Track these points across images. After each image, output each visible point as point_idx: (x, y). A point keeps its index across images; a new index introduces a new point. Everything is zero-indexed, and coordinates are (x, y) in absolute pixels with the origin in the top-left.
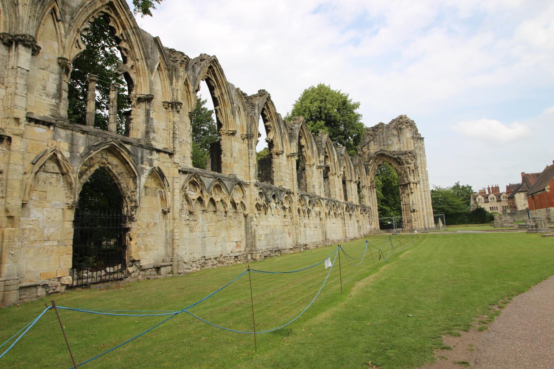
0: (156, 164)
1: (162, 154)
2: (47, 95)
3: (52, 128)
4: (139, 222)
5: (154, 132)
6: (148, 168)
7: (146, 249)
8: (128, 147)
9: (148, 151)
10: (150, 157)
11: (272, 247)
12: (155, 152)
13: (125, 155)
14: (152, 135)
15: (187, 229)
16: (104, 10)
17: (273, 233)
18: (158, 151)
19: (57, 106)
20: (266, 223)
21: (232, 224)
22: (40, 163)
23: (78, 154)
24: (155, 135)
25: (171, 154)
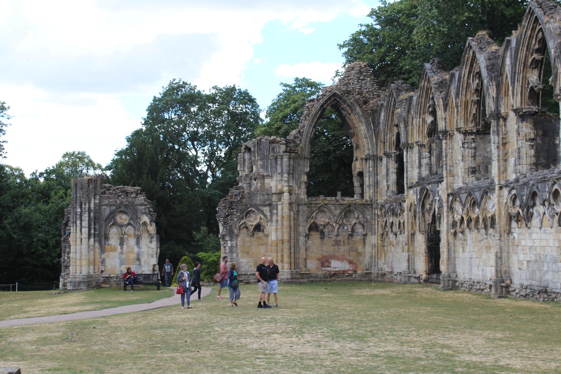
11: (538, 284)
17: (539, 261)
20: (529, 243)
21: (491, 245)
22: (413, 209)
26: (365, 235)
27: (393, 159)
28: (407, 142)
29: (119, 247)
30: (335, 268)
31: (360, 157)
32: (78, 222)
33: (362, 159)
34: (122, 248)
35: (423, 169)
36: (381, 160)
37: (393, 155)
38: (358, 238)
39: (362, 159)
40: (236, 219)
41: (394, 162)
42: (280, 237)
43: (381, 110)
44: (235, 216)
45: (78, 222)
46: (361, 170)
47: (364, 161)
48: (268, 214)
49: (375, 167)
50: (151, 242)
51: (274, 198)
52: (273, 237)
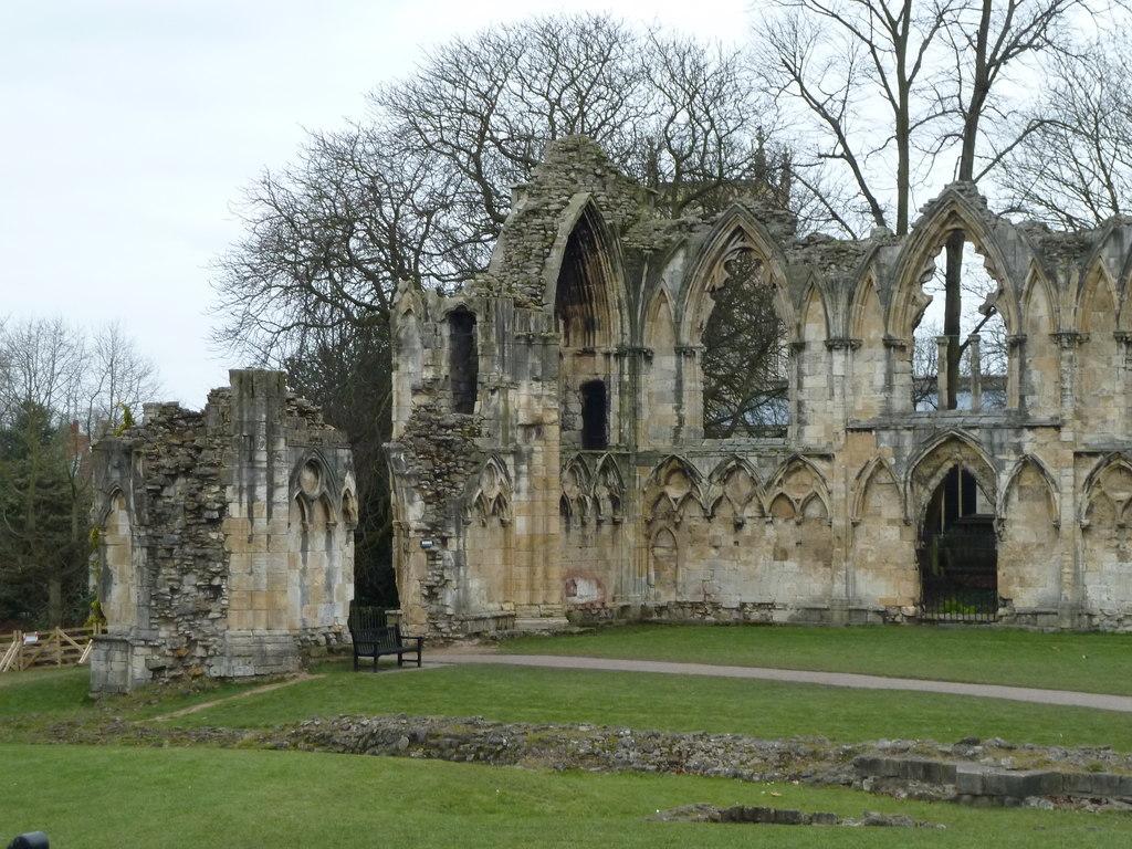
0: (1028, 449)
1: (1040, 431)
2: (875, 391)
3: (874, 433)
4: (1009, 542)
5: (1033, 393)
6: (1013, 457)
7: (1022, 582)
8: (975, 433)
9: (1011, 432)
10: (1016, 441)
12: (1026, 430)
13: (972, 444)
14: (1029, 400)
15: (1114, 556)
16: (949, 227)
18: (1032, 428)
19: (887, 400)
23: (905, 459)
24: (1036, 398)
25: (1058, 428)
26: (616, 523)
27: (698, 360)
28: (847, 334)
29: (300, 555)
30: (582, 597)
31: (603, 349)
32: (261, 491)
33: (607, 355)
34: (304, 561)
35: (897, 393)
36: (648, 357)
37: (698, 353)
38: (606, 529)
39: (607, 355)
40: (462, 485)
41: (698, 368)
42: (539, 530)
43: (674, 255)
44: (460, 478)
45: (261, 491)
46: (601, 378)
47: (612, 358)
48: (512, 474)
49: (634, 373)
50: (347, 543)
51: (519, 435)
52: (521, 524)
